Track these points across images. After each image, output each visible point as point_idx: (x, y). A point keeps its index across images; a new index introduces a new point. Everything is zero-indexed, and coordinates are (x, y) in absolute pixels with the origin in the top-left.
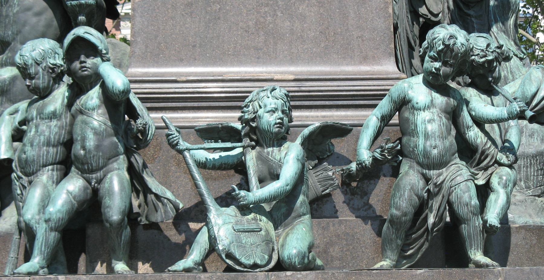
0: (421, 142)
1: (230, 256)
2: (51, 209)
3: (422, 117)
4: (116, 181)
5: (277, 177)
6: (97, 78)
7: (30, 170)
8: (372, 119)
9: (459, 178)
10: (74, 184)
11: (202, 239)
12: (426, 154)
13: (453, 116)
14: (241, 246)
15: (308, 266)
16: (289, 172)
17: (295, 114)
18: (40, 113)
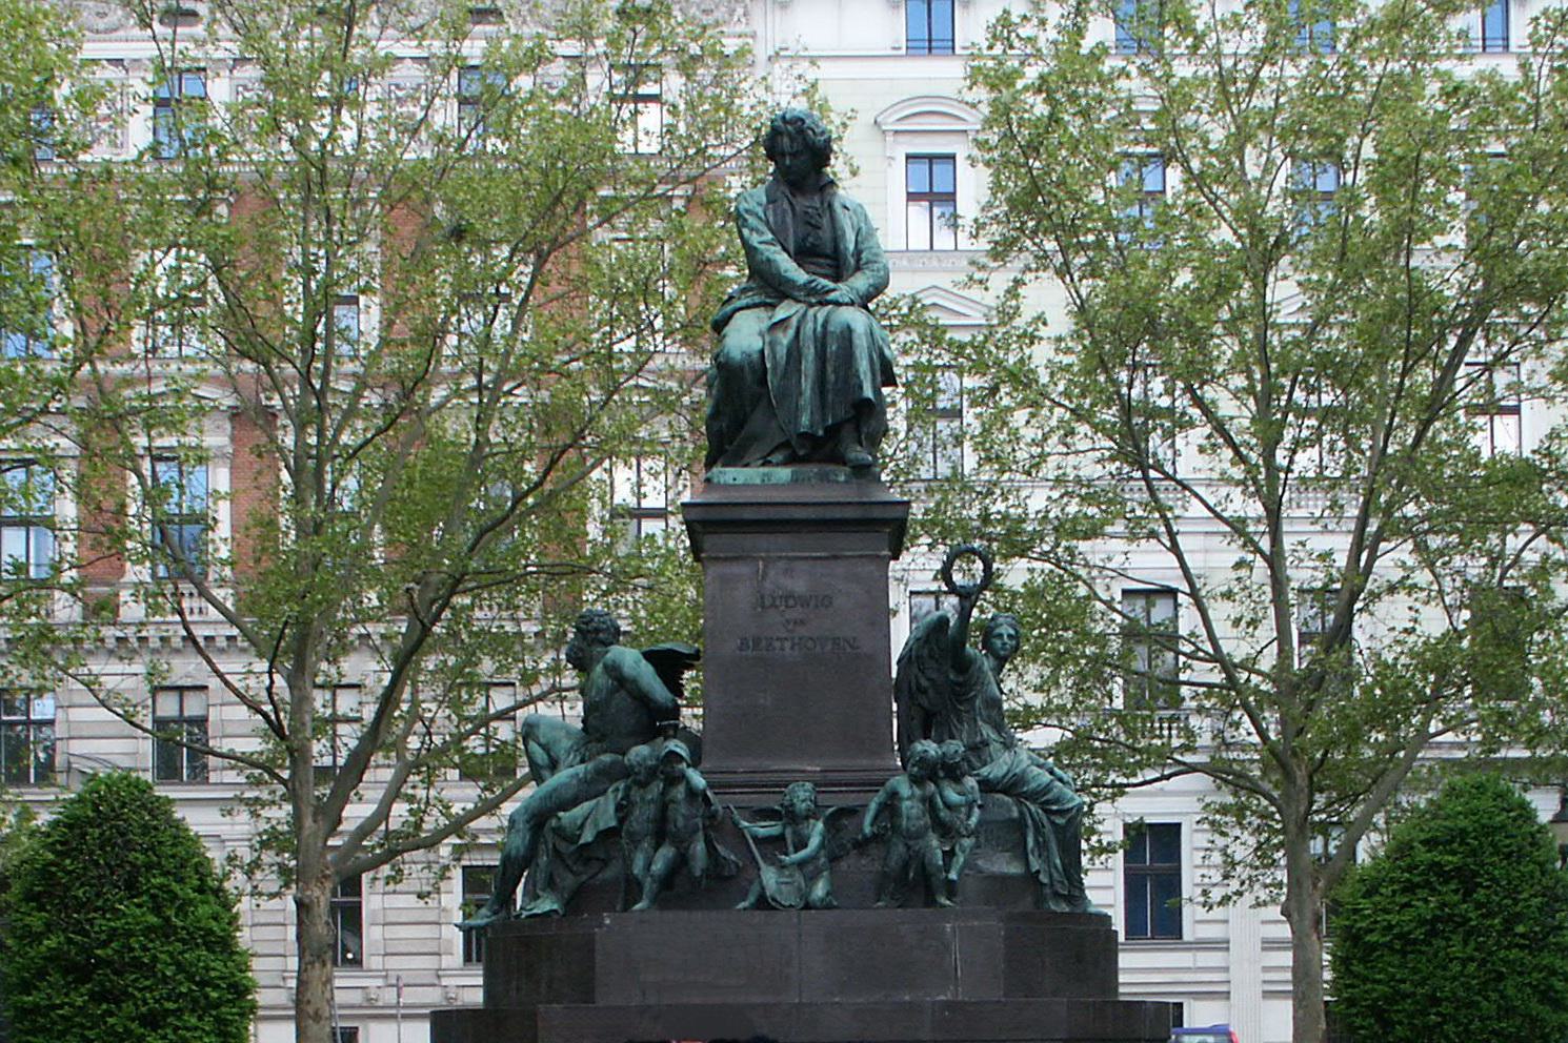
0: (904, 822)
1: (774, 900)
2: (653, 868)
3: (906, 804)
4: (699, 847)
5: (806, 846)
6: (683, 777)
7: (635, 841)
8: (873, 806)
9: (935, 845)
10: (666, 853)
11: (755, 889)
12: (908, 830)
13: (929, 802)
14: (781, 893)
15: (829, 907)
16: (814, 842)
17: (820, 797)
18: (642, 799)
